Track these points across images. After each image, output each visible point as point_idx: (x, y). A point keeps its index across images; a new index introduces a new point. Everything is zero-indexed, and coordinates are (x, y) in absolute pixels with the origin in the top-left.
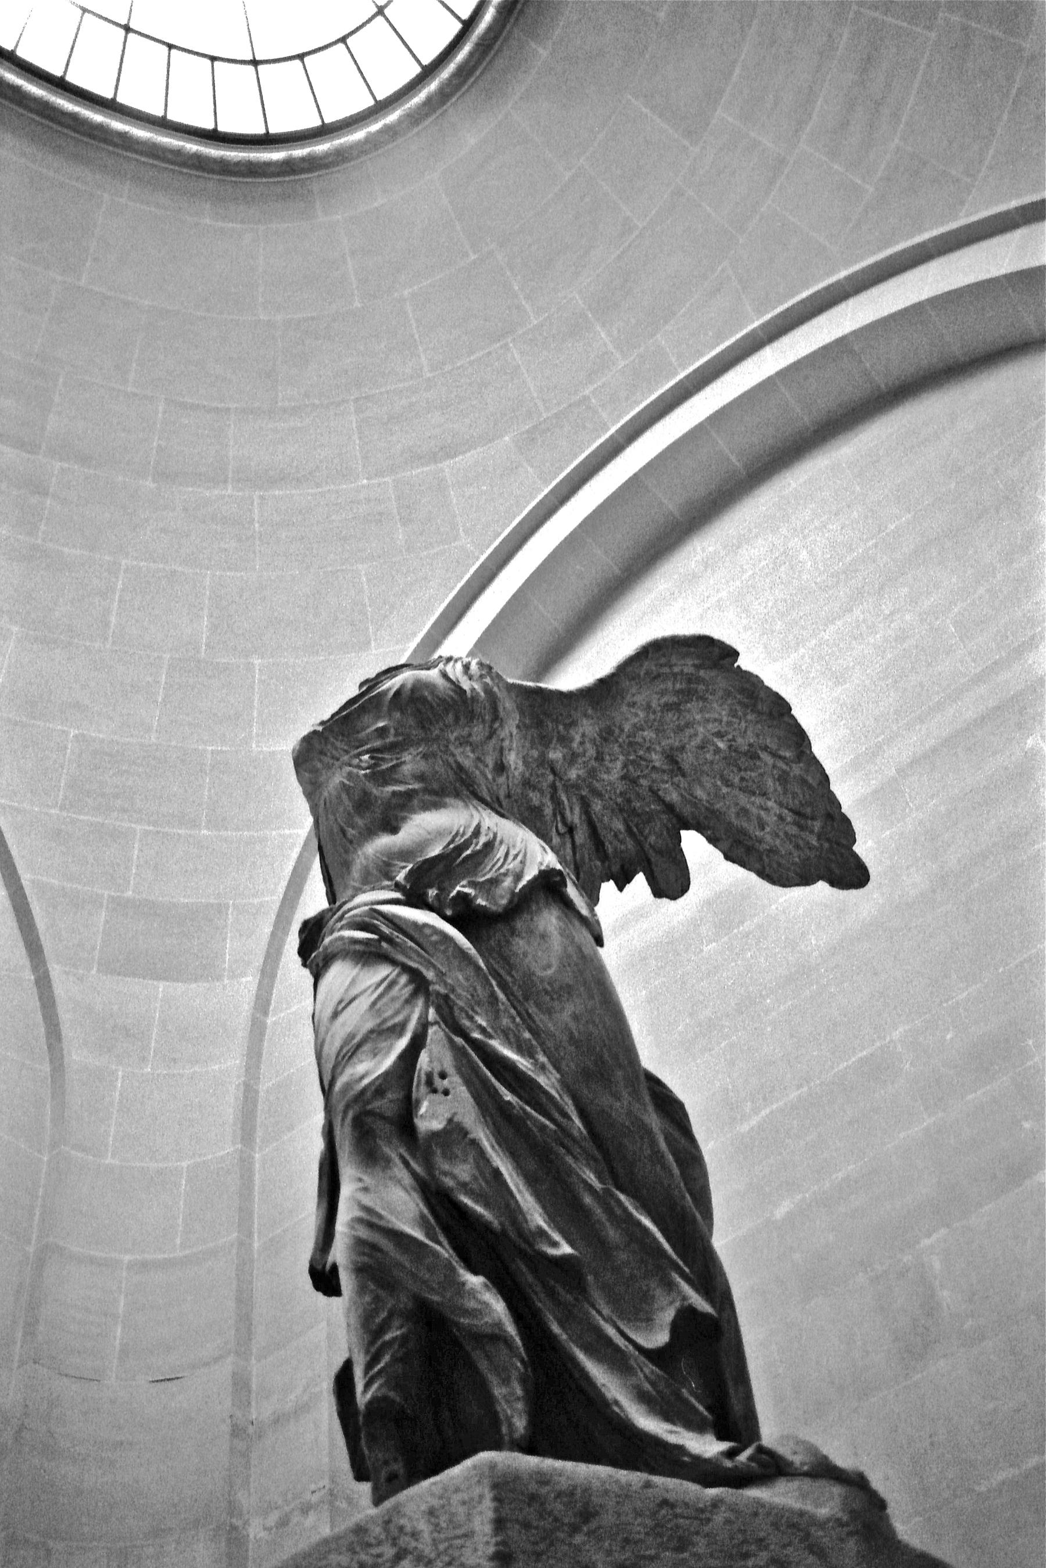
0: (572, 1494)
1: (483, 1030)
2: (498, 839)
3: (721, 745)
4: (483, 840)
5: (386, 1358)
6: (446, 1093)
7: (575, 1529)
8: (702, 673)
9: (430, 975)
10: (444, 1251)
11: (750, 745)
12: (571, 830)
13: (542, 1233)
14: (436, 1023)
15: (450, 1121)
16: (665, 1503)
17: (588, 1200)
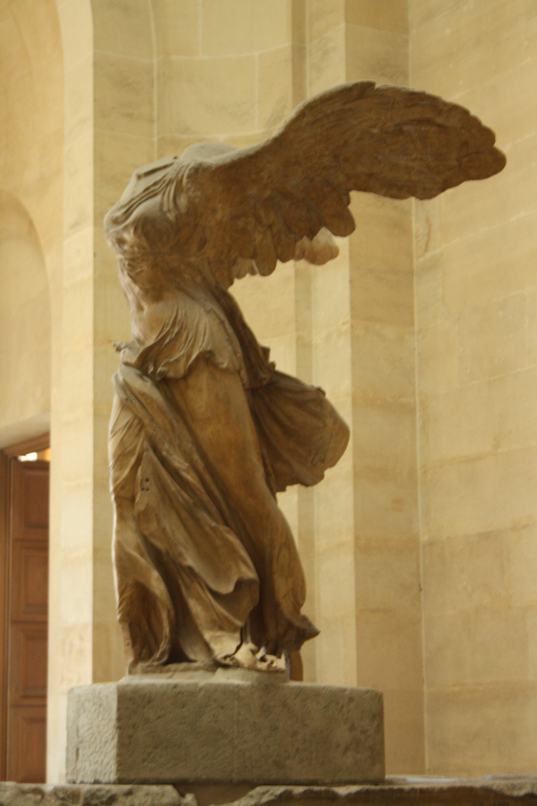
0: (145, 695)
1: (168, 452)
2: (184, 327)
3: (375, 131)
4: (176, 330)
5: (124, 604)
6: (147, 489)
7: (144, 707)
8: (348, 106)
9: (146, 421)
10: (144, 562)
11: (396, 126)
12: (270, 227)
13: (180, 554)
14: (147, 450)
15: (148, 505)
16: (180, 693)
17: (207, 529)
